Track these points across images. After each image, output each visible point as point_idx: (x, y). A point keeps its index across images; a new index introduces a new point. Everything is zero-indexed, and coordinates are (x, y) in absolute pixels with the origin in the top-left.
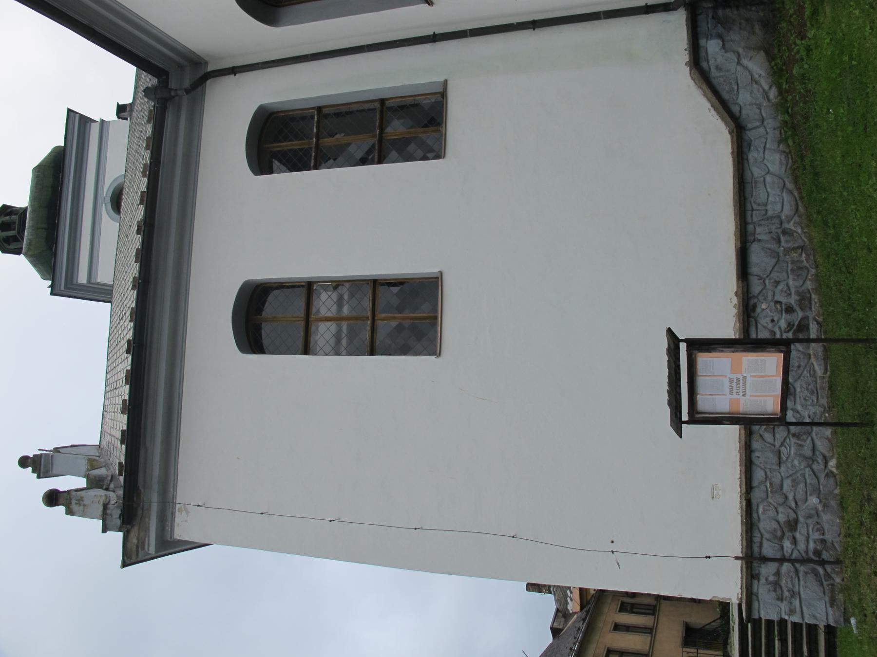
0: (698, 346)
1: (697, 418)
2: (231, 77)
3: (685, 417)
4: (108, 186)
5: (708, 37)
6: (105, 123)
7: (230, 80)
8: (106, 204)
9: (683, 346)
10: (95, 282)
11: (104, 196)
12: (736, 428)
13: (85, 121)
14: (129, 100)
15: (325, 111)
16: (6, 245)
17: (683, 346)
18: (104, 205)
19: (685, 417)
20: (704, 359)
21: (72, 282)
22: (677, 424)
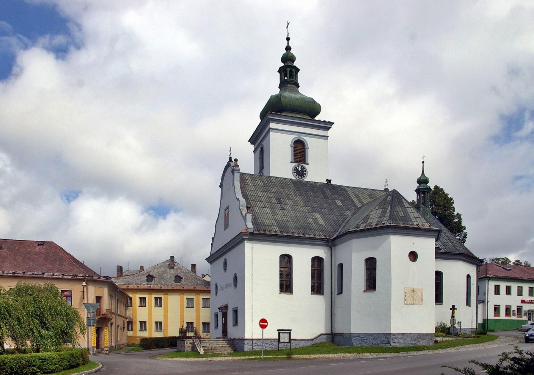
0: (290, 333)
1: (279, 333)
2: (330, 253)
3: (279, 331)
4: (304, 138)
5: (327, 336)
6: (327, 138)
7: (330, 251)
8: (298, 137)
9: (290, 331)
10: (270, 131)
11: (301, 137)
12: (278, 338)
13: (328, 129)
14: (332, 183)
15: (322, 271)
16: (283, 70)
17: (290, 331)
18: (297, 136)
19: (279, 331)
20: (288, 334)
21: (270, 120)
22: (278, 330)
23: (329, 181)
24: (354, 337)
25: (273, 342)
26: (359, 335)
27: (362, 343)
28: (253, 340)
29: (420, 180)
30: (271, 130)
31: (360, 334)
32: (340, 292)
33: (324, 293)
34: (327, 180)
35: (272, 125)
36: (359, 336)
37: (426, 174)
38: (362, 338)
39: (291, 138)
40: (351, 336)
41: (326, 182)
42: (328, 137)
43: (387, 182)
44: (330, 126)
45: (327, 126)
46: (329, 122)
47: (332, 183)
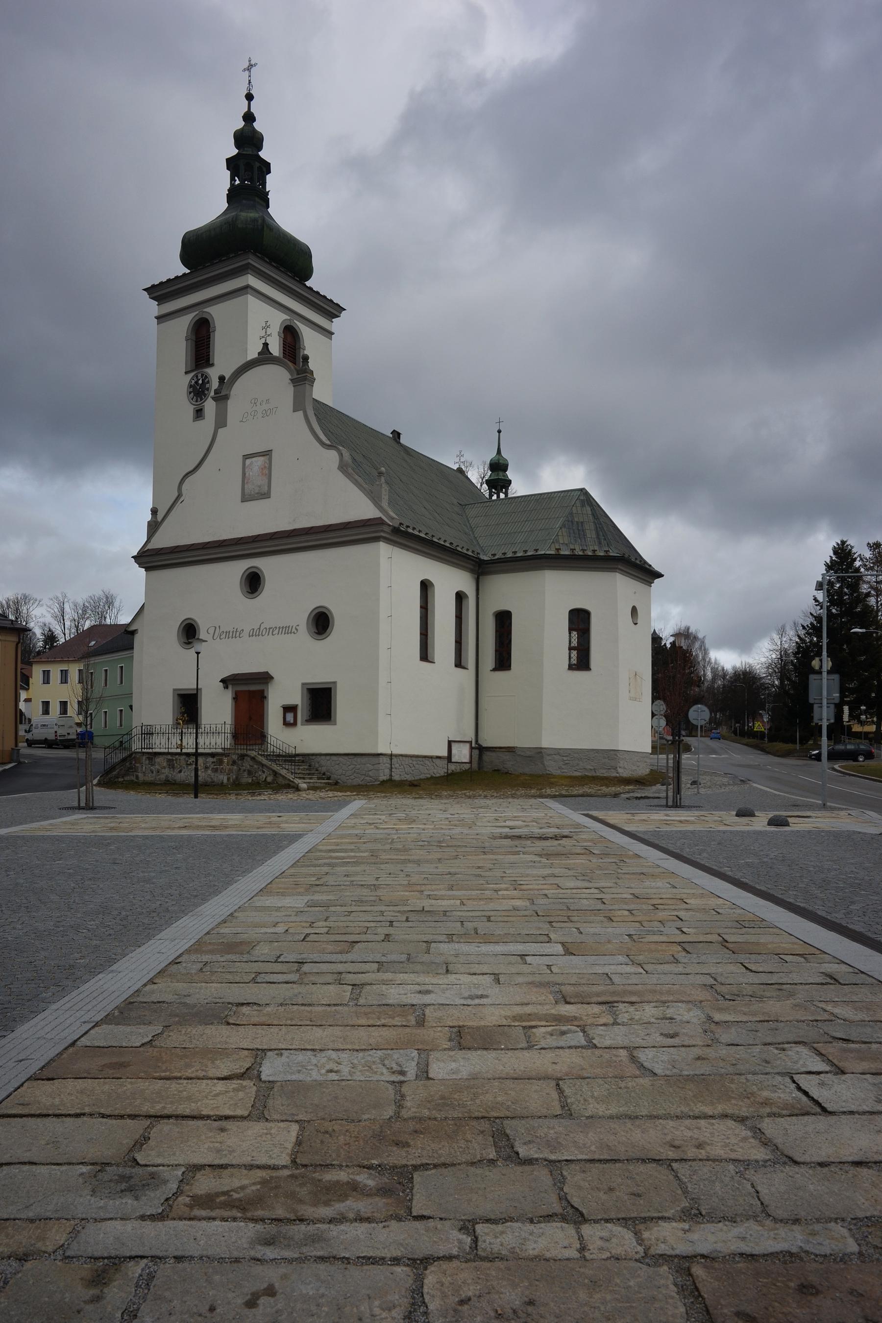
8: (290, 320)
23: (397, 435)
24: (549, 755)
25: (438, 761)
26: (558, 752)
27: (563, 767)
28: (391, 756)
29: (496, 463)
30: (249, 290)
31: (560, 749)
32: (503, 662)
33: (433, 658)
34: (394, 432)
35: (252, 280)
36: (559, 754)
37: (504, 454)
38: (565, 758)
39: (278, 319)
40: (541, 752)
41: (391, 436)
42: (333, 334)
43: (463, 456)
44: (338, 314)
45: (331, 310)
46: (338, 305)
47: (402, 441)
